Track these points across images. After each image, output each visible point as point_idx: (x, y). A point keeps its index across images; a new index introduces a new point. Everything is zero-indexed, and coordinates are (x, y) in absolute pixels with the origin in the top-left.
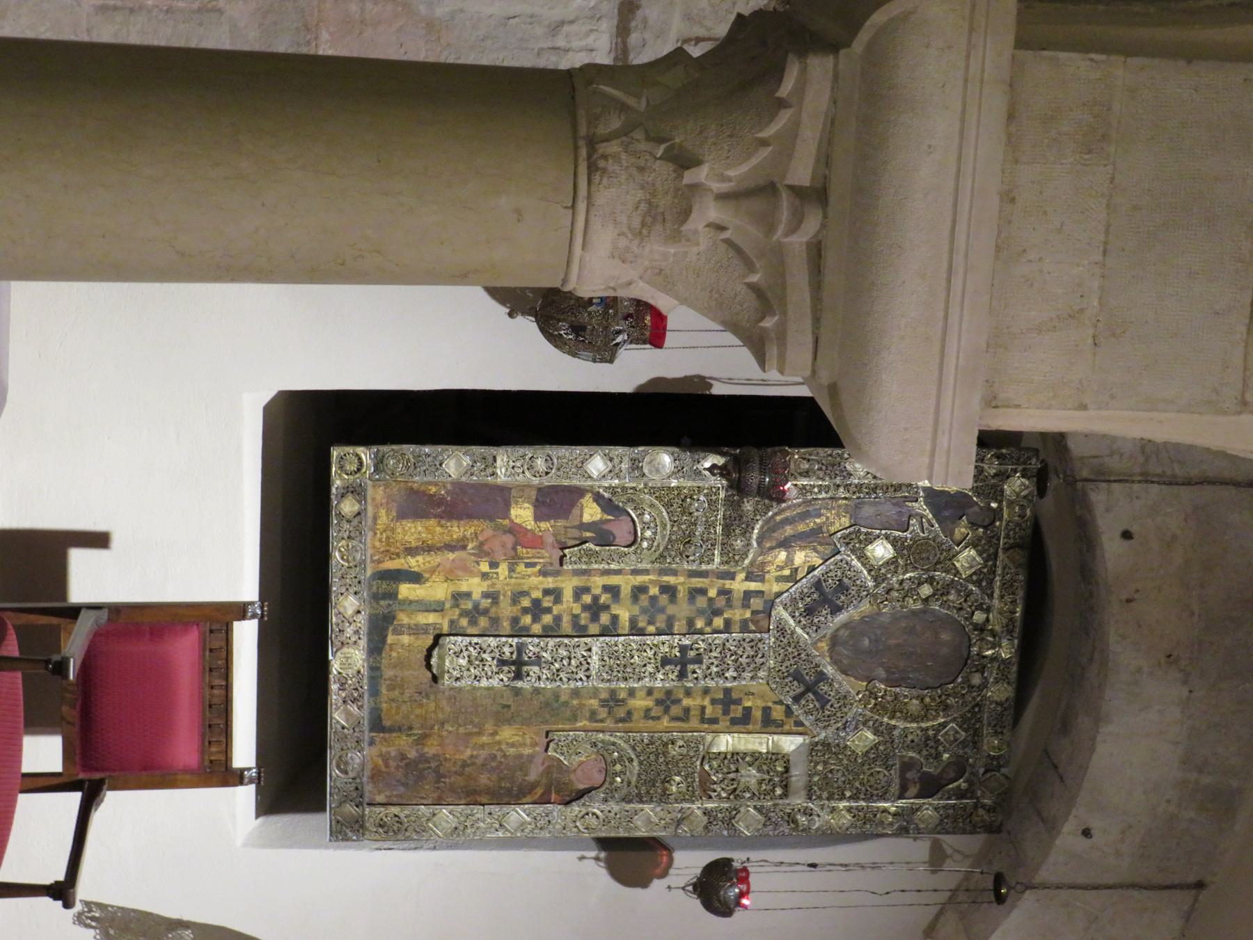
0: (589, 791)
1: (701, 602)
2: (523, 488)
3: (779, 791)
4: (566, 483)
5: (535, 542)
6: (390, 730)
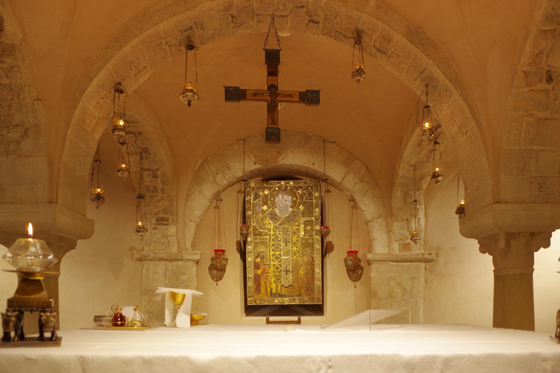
2: (254, 272)
3: (311, 222)
4: (253, 265)
5: (264, 270)
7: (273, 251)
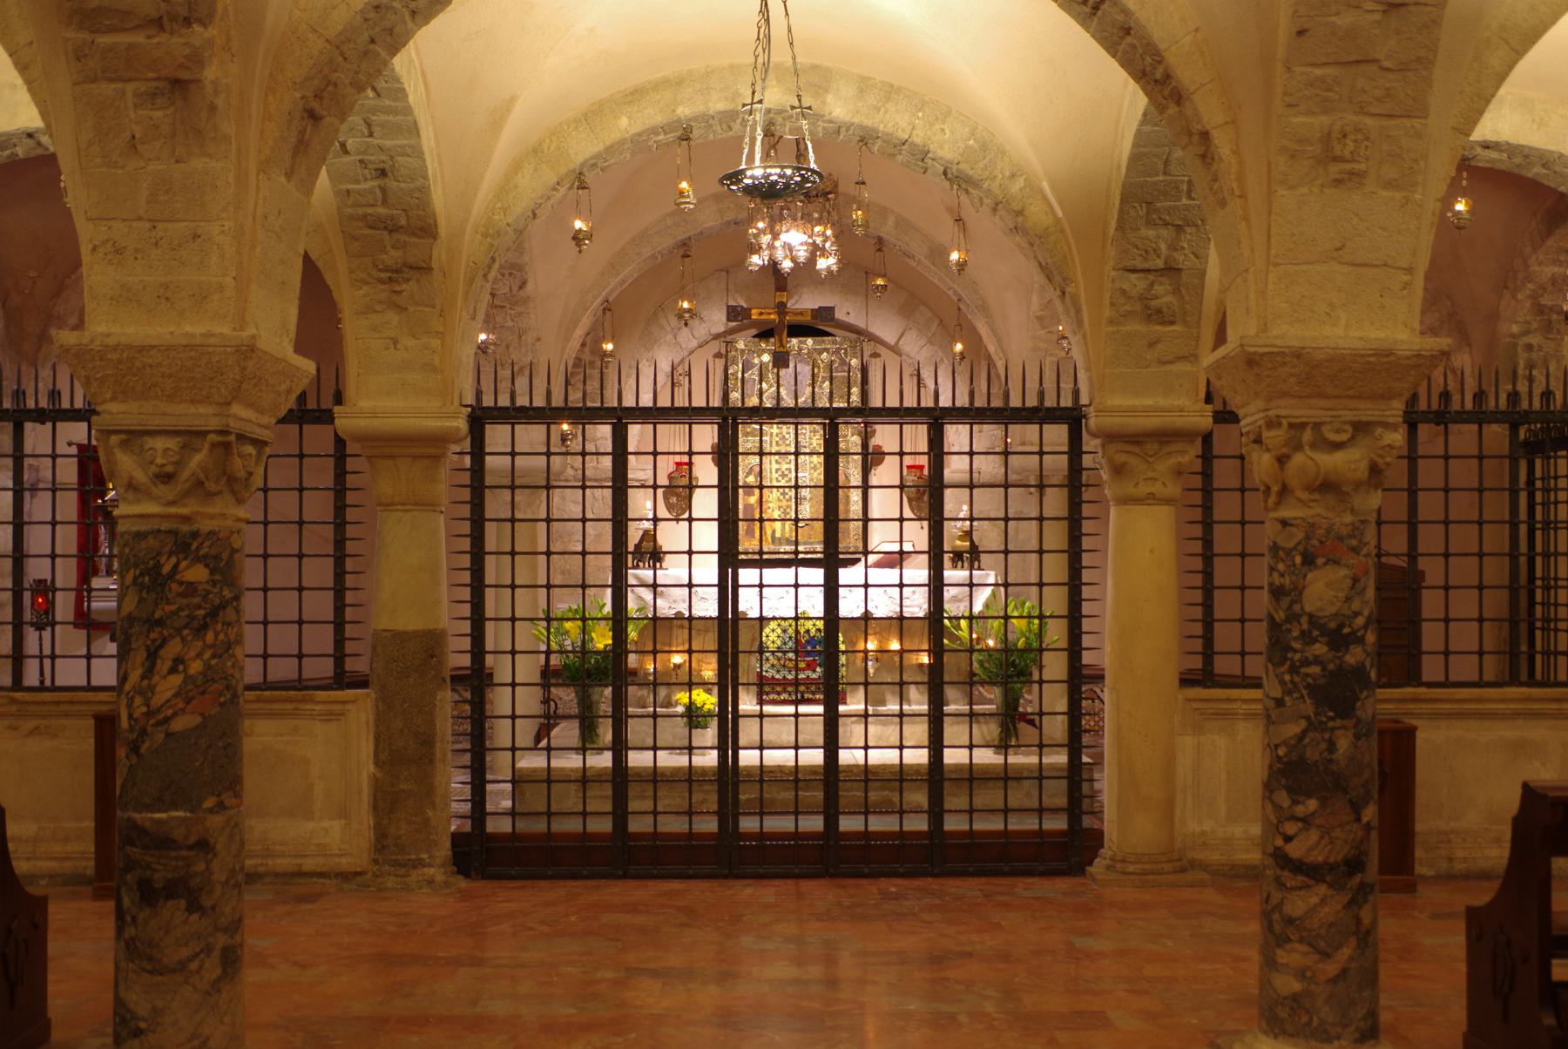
1: (780, 442)
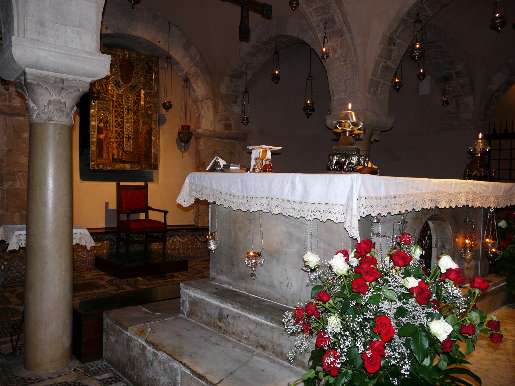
0: (150, 127)
1: (118, 106)
4: (96, 129)
6: (140, 160)
7: (115, 117)
